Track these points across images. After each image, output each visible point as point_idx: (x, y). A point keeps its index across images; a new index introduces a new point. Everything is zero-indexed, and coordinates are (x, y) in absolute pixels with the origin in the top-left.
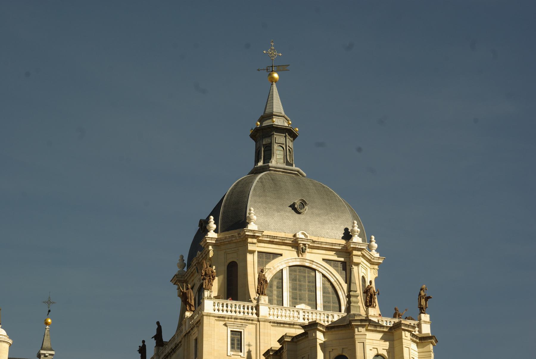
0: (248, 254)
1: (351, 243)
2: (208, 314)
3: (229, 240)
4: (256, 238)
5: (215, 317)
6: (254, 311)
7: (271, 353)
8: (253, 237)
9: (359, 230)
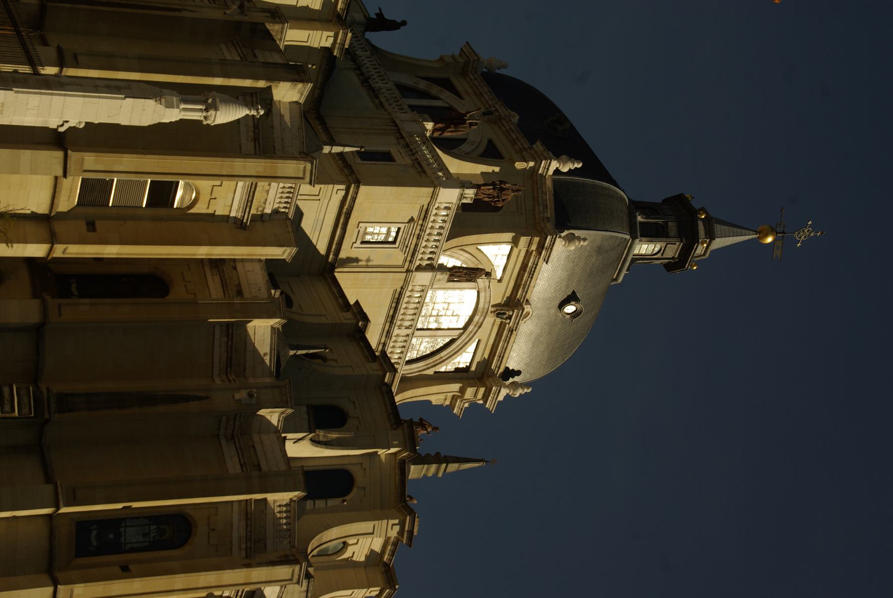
0: (514, 234)
1: (499, 388)
2: (436, 195)
4: (537, 249)
5: (429, 204)
6: (424, 263)
7: (360, 323)
8: (541, 247)
9: (517, 395)
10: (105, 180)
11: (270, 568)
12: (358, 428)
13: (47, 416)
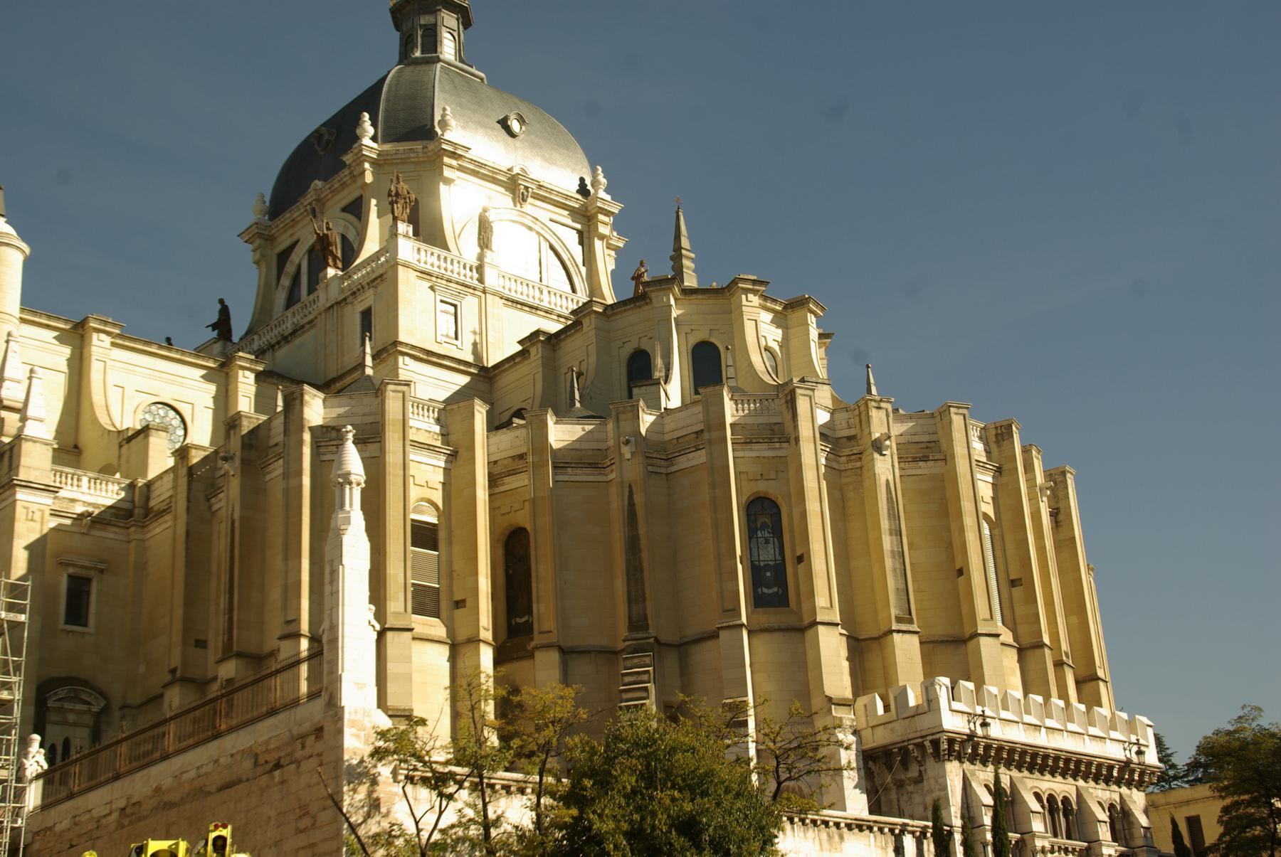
3: (403, 157)
4: (456, 159)
6: (476, 275)
7: (542, 338)
8: (454, 155)
10: (413, 592)
11: (799, 418)
12: (651, 338)
13: (652, 640)
